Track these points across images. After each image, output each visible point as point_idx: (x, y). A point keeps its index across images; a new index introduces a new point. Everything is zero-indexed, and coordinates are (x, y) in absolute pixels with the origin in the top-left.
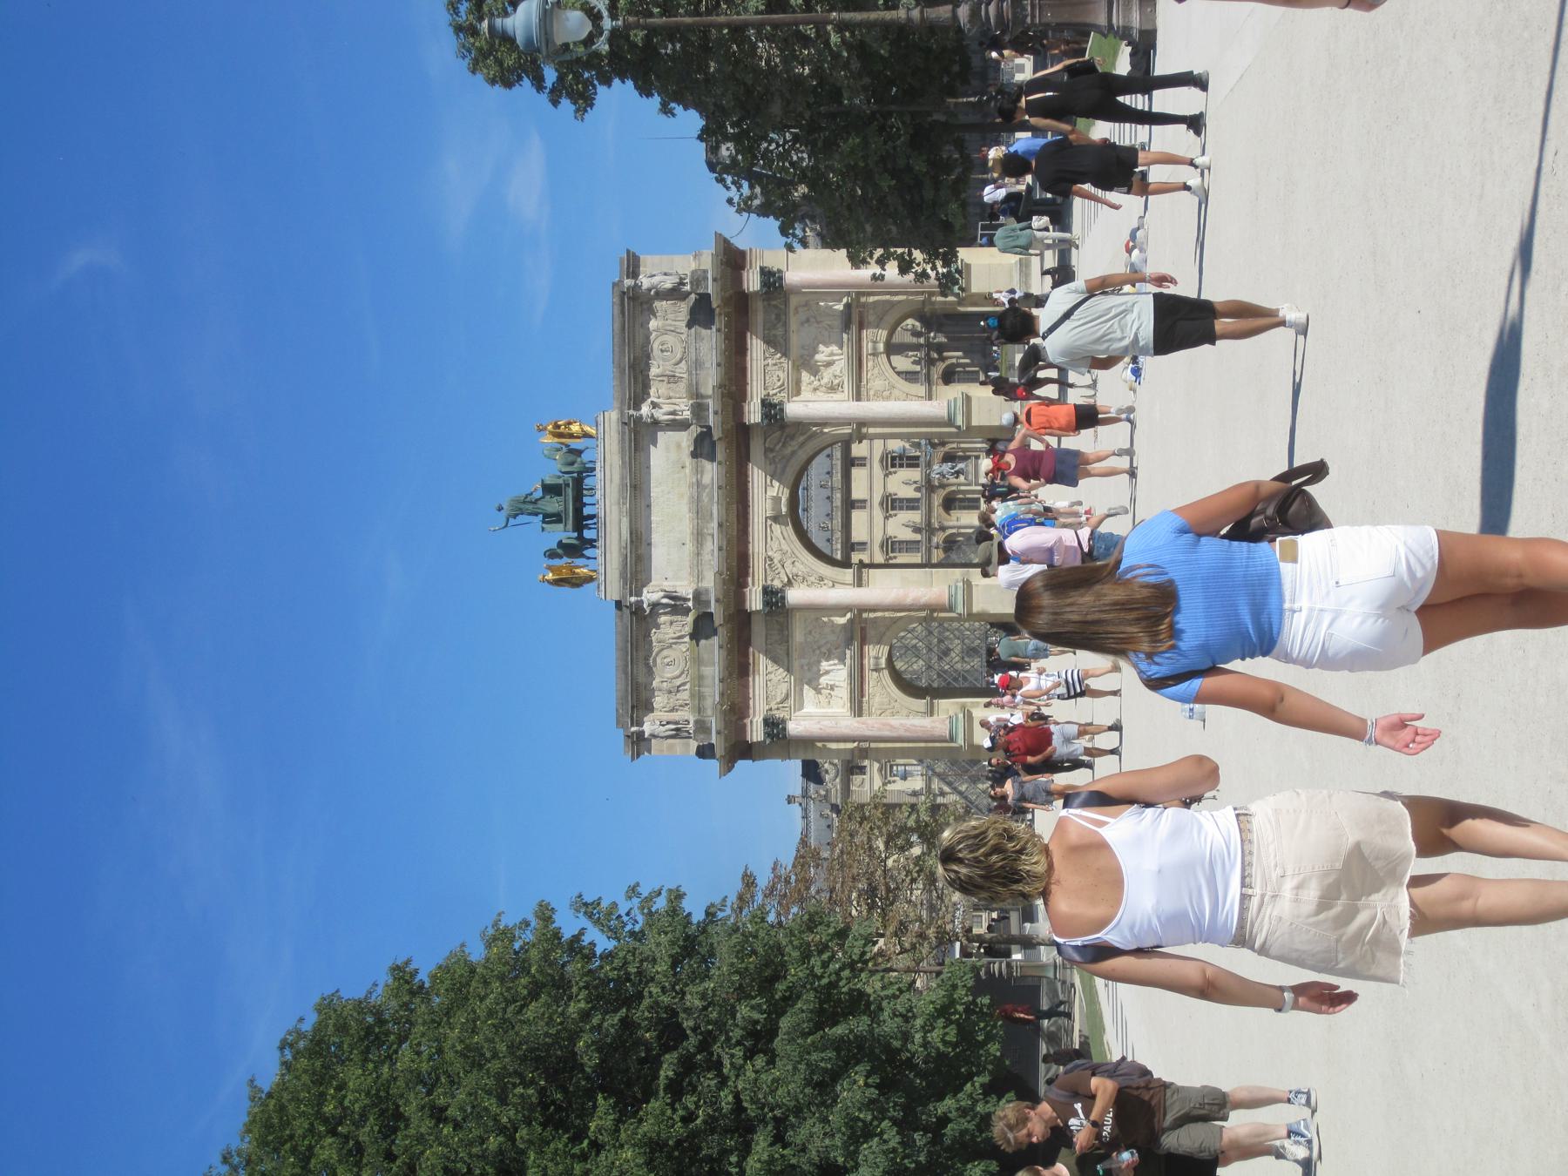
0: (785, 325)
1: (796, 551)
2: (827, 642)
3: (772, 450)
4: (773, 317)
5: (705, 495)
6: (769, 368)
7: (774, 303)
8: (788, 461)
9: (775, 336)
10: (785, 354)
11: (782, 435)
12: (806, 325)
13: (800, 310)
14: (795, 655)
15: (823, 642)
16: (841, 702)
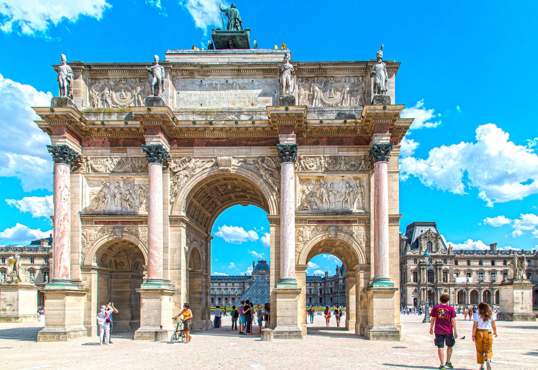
0: (348, 171)
1: (194, 177)
2: (133, 199)
3: (263, 161)
4: (353, 163)
5: (233, 117)
6: (318, 160)
7: (363, 162)
8: (256, 173)
9: (340, 164)
10: (327, 170)
11: (274, 168)
12: (347, 185)
13: (358, 181)
14: (125, 177)
15: (135, 197)
16: (94, 208)
